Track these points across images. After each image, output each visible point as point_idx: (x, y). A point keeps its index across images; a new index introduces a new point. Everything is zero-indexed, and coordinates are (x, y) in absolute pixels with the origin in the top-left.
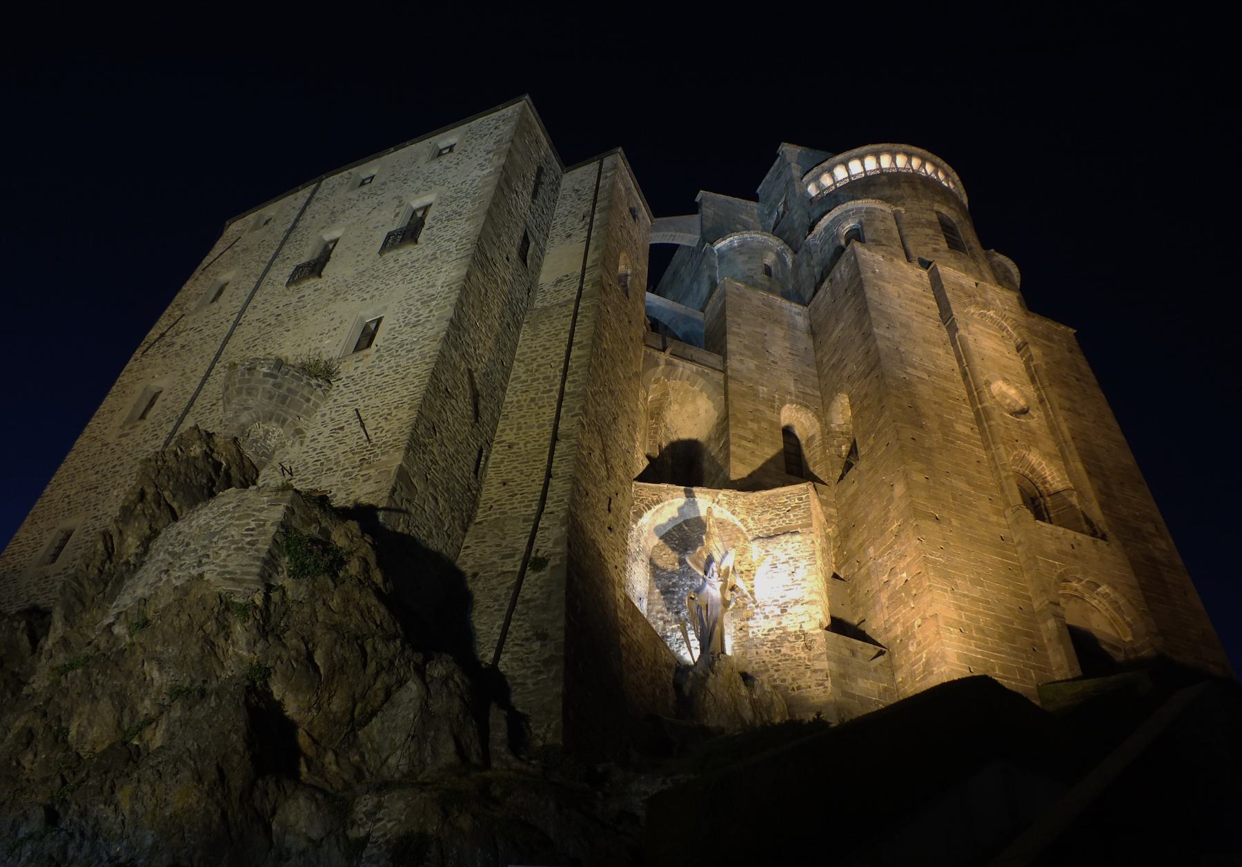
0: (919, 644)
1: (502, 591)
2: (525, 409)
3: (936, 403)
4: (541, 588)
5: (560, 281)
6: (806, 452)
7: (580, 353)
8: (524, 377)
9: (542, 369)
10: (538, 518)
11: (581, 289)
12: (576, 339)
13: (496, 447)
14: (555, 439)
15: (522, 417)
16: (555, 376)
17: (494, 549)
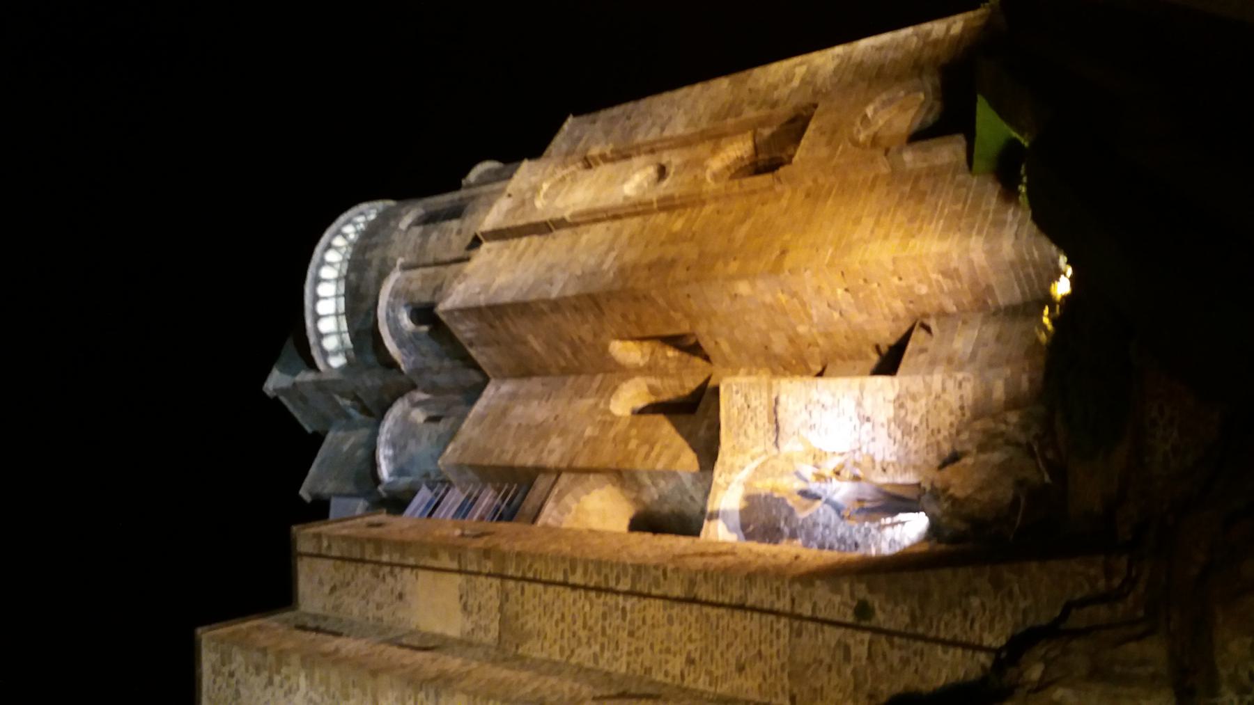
0: (920, 281)
1: (895, 656)
2: (642, 644)
3: (646, 246)
4: (896, 604)
5: (465, 607)
6: (666, 397)
7: (580, 571)
8: (597, 648)
9: (591, 622)
10: (800, 617)
11: (489, 575)
12: (560, 577)
13: (688, 682)
14: (693, 600)
15: (652, 647)
16: (605, 604)
17: (834, 673)
